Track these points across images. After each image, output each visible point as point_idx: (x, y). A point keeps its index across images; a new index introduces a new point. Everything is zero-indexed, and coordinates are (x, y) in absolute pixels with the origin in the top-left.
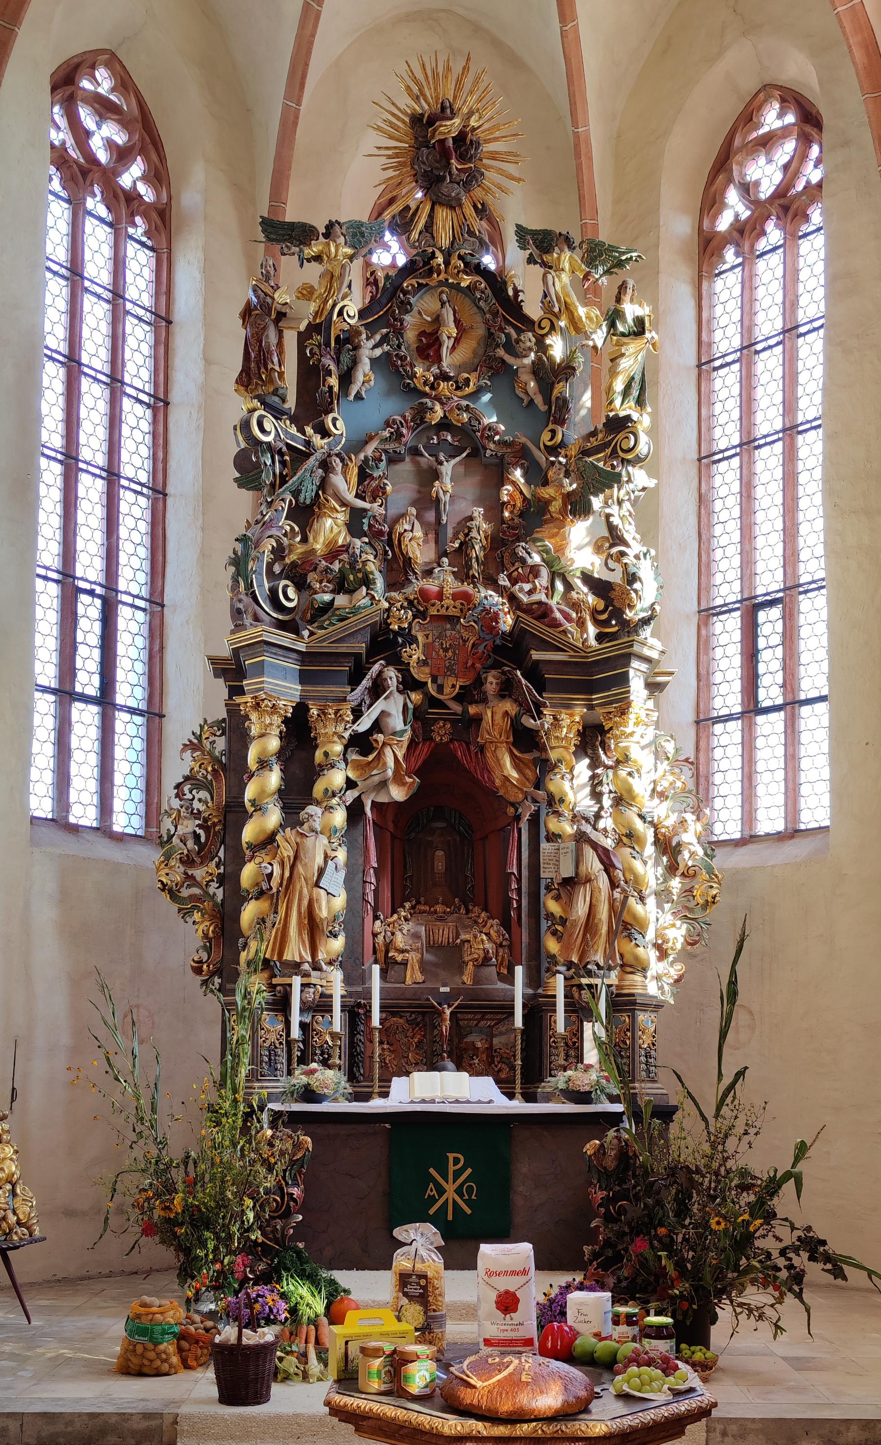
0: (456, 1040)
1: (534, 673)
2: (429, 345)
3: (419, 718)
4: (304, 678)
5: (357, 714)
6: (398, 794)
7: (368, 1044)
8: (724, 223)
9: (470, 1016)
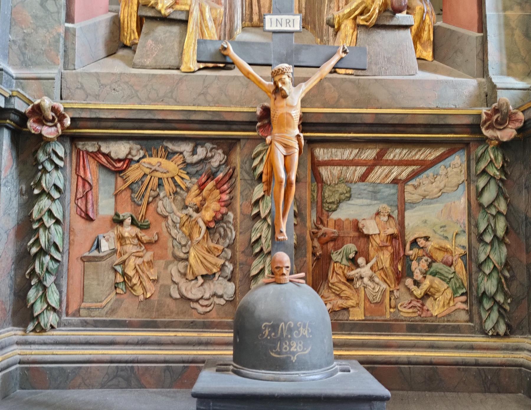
0: (312, 217)
7: (79, 224)
9: (347, 153)
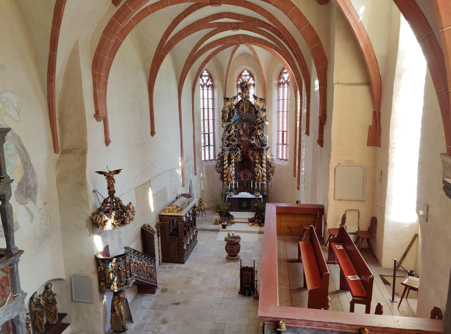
1: (254, 150)
2: (243, 109)
3: (242, 152)
4: (229, 150)
5: (235, 153)
6: (240, 160)
8: (281, 80)
